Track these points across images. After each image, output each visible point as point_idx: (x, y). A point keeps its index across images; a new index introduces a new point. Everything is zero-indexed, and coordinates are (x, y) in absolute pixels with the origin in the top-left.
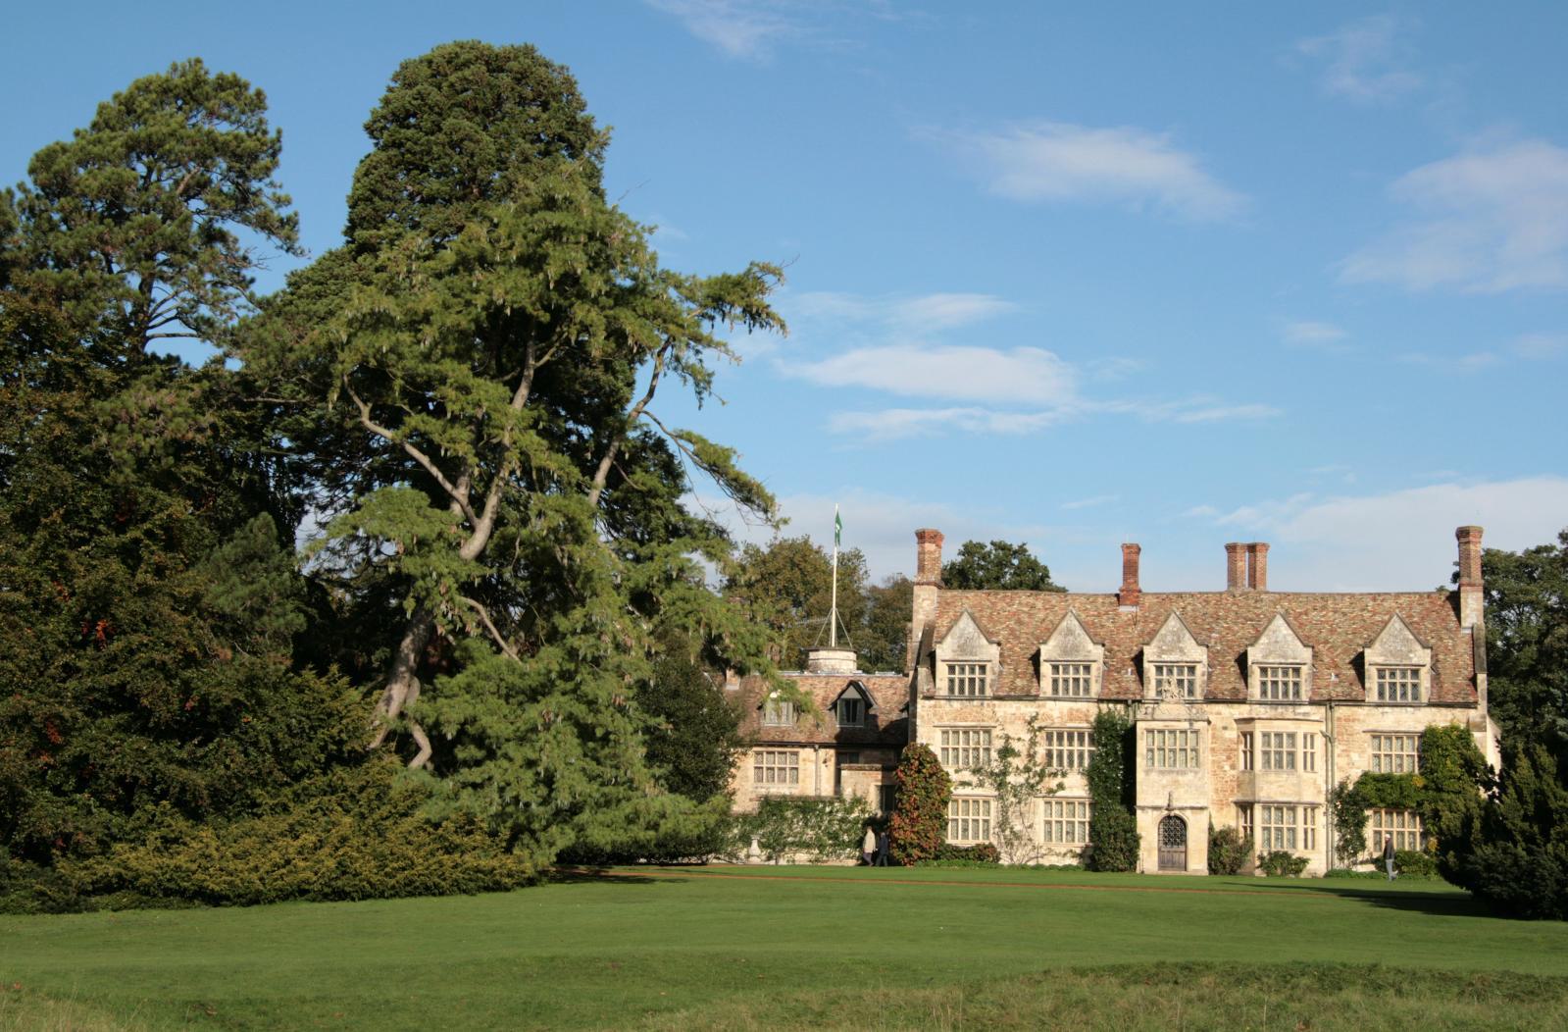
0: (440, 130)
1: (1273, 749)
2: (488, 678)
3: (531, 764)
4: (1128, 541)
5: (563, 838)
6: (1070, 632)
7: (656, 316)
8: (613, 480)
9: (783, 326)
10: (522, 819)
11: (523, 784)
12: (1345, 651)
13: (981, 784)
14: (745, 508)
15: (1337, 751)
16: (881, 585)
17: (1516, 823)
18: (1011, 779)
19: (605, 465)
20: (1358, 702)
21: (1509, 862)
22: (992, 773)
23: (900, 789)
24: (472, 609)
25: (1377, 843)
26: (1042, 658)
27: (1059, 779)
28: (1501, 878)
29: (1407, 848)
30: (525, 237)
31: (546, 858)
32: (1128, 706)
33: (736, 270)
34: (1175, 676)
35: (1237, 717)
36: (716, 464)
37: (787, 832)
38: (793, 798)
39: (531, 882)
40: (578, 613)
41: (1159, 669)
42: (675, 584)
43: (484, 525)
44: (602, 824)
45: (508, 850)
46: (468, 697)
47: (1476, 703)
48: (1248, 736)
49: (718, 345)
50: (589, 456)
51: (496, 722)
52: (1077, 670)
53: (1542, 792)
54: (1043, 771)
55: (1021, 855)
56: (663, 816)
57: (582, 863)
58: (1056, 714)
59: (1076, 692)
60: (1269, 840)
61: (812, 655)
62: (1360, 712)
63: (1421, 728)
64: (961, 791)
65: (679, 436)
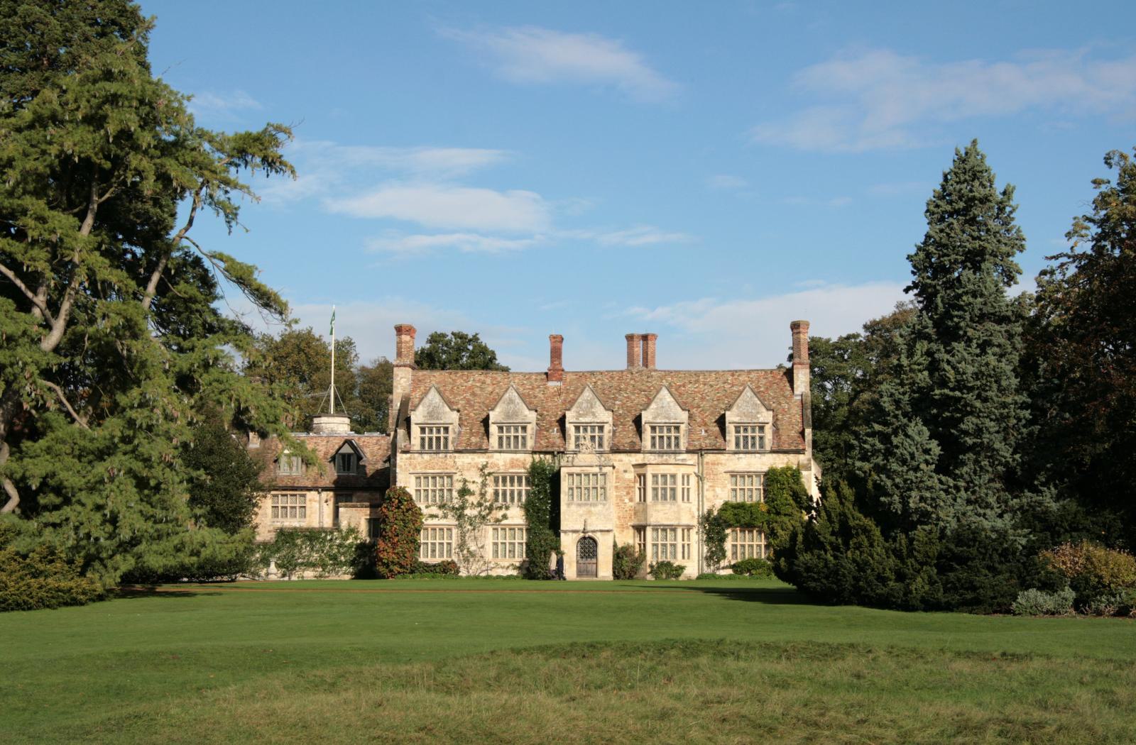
0: (16, 13)
1: (660, 486)
2: (64, 442)
3: (99, 508)
4: (554, 333)
5: (125, 563)
6: (511, 401)
7: (193, 164)
8: (162, 289)
9: (293, 172)
10: (93, 550)
11: (93, 523)
12: (712, 413)
13: (445, 516)
14: (265, 311)
15: (706, 487)
16: (369, 366)
17: (826, 537)
18: (468, 512)
19: (156, 277)
20: (721, 451)
21: (821, 565)
22: (453, 508)
23: (384, 521)
24: (50, 389)
25: (735, 553)
26: (491, 421)
28: (816, 576)
29: (755, 557)
30: (88, 101)
31: (112, 579)
32: (554, 456)
33: (256, 129)
34: (589, 433)
35: (634, 463)
36: (243, 278)
37: (297, 555)
38: (302, 530)
39: (101, 598)
40: (135, 392)
41: (577, 428)
42: (211, 370)
43: (59, 325)
44: (156, 552)
45: (82, 574)
46: (48, 457)
47: (804, 450)
48: (642, 477)
49: (242, 188)
50: (142, 271)
51: (71, 477)
52: (516, 430)
53: (844, 515)
54: (491, 505)
55: (475, 569)
56: (204, 545)
57: (141, 582)
58: (501, 463)
59: (516, 446)
60: (657, 553)
61: (316, 421)
63: (765, 469)
64: (430, 521)
65: (212, 256)
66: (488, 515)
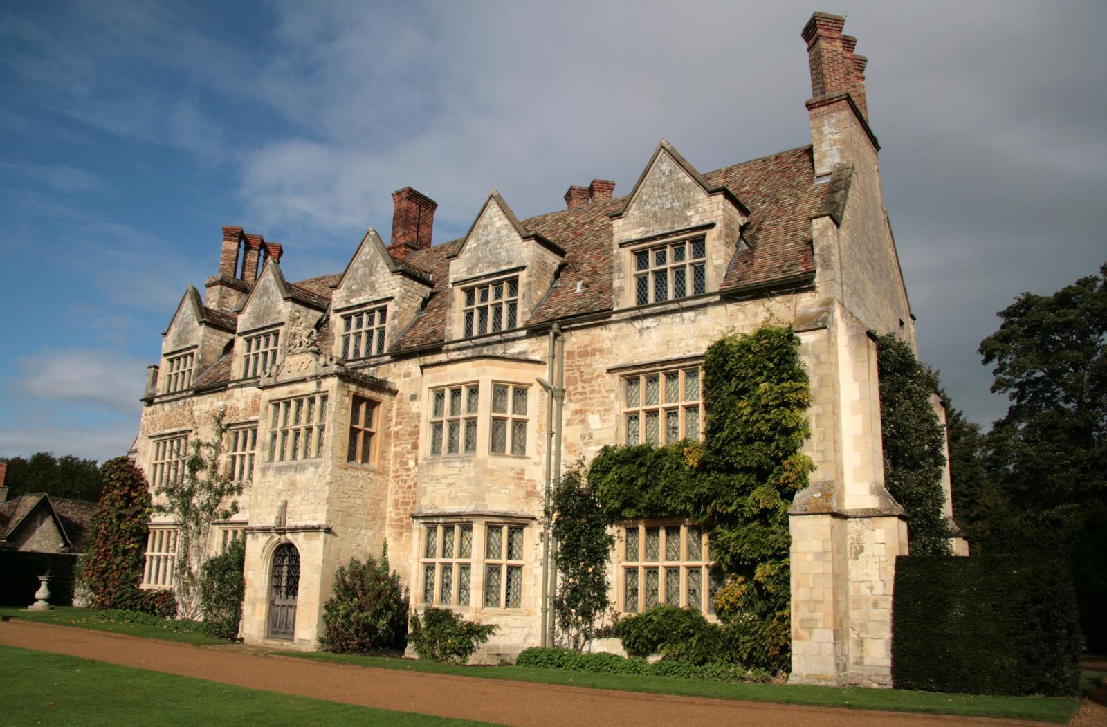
6: (266, 290)
13: (172, 510)
15: (566, 415)
27: (235, 497)
29: (682, 602)
58: (241, 405)
62: (603, 335)
66: (216, 505)
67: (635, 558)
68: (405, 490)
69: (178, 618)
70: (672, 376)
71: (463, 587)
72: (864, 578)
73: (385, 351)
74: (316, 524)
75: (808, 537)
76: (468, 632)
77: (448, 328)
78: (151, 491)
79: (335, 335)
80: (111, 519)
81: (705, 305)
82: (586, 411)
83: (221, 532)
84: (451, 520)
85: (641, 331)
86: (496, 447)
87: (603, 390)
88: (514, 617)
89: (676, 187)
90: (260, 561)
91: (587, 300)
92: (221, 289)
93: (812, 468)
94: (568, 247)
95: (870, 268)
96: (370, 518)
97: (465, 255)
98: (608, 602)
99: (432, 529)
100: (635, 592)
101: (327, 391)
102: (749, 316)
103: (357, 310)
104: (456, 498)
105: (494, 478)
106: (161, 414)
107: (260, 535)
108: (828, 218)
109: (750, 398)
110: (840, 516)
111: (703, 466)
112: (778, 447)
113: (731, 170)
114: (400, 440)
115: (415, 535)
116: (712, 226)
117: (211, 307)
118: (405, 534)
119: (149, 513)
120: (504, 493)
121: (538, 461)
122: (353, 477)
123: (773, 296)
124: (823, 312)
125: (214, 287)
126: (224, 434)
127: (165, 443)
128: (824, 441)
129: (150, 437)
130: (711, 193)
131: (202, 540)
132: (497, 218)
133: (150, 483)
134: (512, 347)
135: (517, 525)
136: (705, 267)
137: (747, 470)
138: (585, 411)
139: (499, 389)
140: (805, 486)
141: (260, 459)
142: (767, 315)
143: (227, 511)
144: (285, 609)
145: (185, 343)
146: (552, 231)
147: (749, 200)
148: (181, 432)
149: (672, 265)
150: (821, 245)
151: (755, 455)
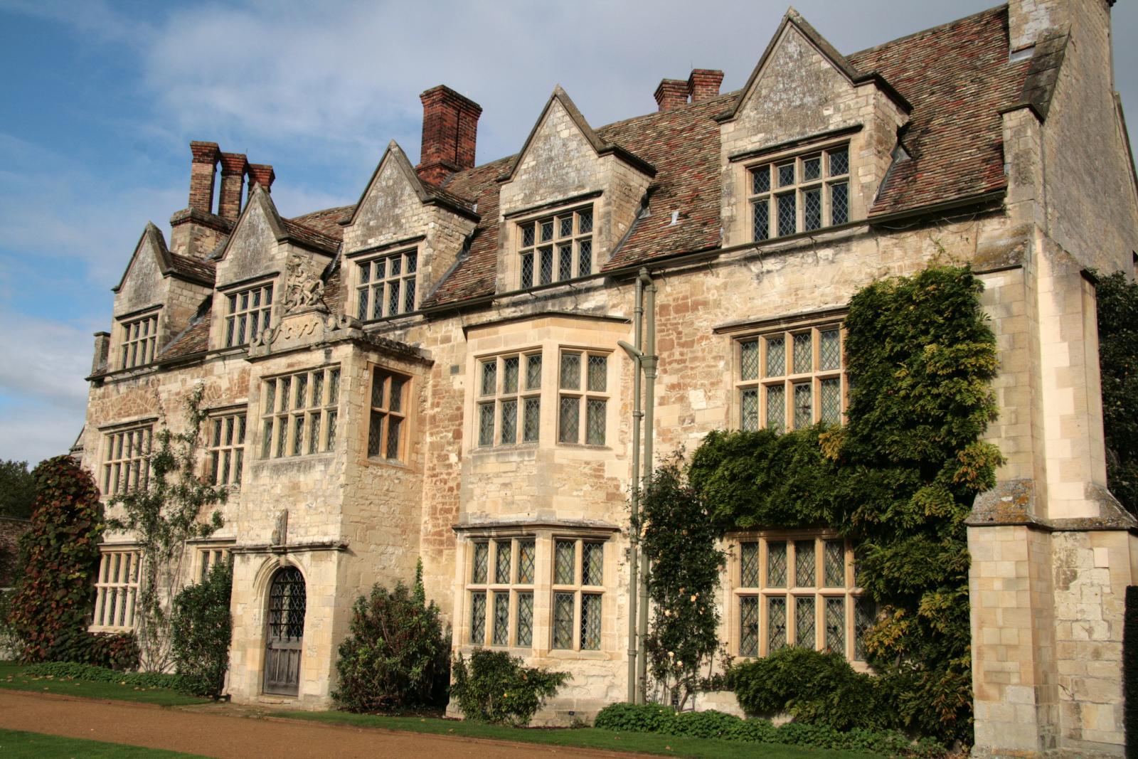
6: (253, 229)
13: (132, 525)
15: (659, 390)
27: (218, 506)
29: (819, 644)
58: (224, 384)
62: (709, 283)
66: (193, 518)
67: (753, 583)
68: (445, 493)
69: (142, 670)
70: (802, 337)
71: (524, 622)
72: (1079, 616)
73: (416, 308)
74: (326, 540)
75: (994, 557)
76: (531, 683)
77: (500, 276)
78: (104, 500)
79: (349, 288)
80: (48, 540)
81: (848, 239)
82: (686, 385)
83: (200, 554)
84: (506, 533)
85: (759, 277)
86: (566, 434)
87: (709, 357)
88: (591, 662)
89: (807, 76)
90: (253, 590)
91: (686, 236)
92: (193, 228)
93: (999, 461)
94: (660, 163)
95: (1088, 179)
96: (398, 531)
97: (521, 178)
98: (717, 643)
99: (481, 545)
100: (754, 628)
101: (339, 363)
102: (910, 253)
103: (378, 254)
104: (513, 503)
105: (564, 476)
106: (114, 397)
107: (252, 556)
108: (1026, 111)
109: (910, 365)
110: (1044, 529)
111: (846, 459)
112: (950, 432)
113: (886, 48)
114: (438, 426)
115: (460, 552)
116: (858, 128)
117: (180, 253)
118: (446, 552)
119: (101, 531)
120: (578, 496)
121: (620, 452)
122: (376, 476)
123: (944, 224)
124: (1016, 244)
125: (182, 226)
126: (201, 423)
127: (121, 436)
128: (1016, 423)
129: (101, 429)
130: (858, 82)
131: (173, 565)
132: (562, 127)
133: (102, 490)
134: (586, 301)
135: (595, 538)
136: (849, 186)
137: (907, 464)
138: (685, 385)
139: (569, 357)
140: (990, 485)
141: (251, 455)
142: (935, 251)
143: (207, 526)
144: (287, 655)
145: (145, 302)
146: (638, 142)
147: (913, 90)
148: (143, 421)
149: (802, 185)
150: (1015, 150)
151: (917, 443)
